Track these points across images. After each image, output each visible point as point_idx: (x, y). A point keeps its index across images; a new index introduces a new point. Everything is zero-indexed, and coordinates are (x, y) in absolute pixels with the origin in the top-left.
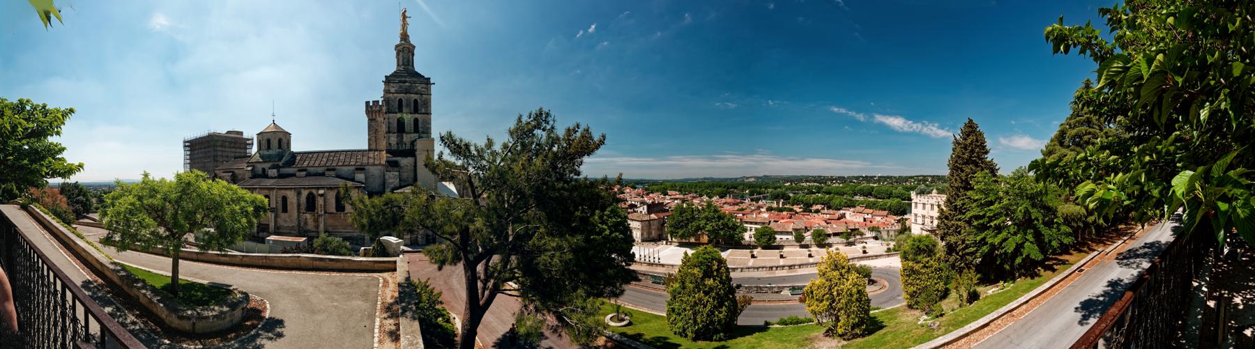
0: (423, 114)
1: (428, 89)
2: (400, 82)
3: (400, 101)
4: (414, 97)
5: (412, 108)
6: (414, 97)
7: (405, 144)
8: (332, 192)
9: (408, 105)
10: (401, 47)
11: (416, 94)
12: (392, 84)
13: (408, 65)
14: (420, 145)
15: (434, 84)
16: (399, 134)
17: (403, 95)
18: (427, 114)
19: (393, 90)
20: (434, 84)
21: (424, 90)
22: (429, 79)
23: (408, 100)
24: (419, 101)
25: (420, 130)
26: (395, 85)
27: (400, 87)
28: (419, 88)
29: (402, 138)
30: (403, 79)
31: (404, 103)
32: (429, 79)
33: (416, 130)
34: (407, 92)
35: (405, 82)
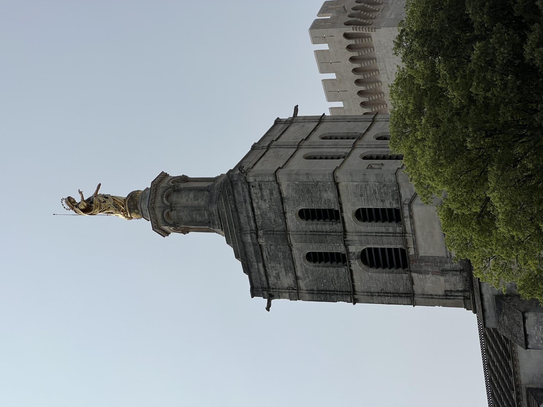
3: (312, 257)
12: (272, 280)
17: (295, 252)
19: (287, 281)
21: (266, 193)
25: (389, 204)
26: (272, 273)
28: (265, 206)
30: (251, 250)
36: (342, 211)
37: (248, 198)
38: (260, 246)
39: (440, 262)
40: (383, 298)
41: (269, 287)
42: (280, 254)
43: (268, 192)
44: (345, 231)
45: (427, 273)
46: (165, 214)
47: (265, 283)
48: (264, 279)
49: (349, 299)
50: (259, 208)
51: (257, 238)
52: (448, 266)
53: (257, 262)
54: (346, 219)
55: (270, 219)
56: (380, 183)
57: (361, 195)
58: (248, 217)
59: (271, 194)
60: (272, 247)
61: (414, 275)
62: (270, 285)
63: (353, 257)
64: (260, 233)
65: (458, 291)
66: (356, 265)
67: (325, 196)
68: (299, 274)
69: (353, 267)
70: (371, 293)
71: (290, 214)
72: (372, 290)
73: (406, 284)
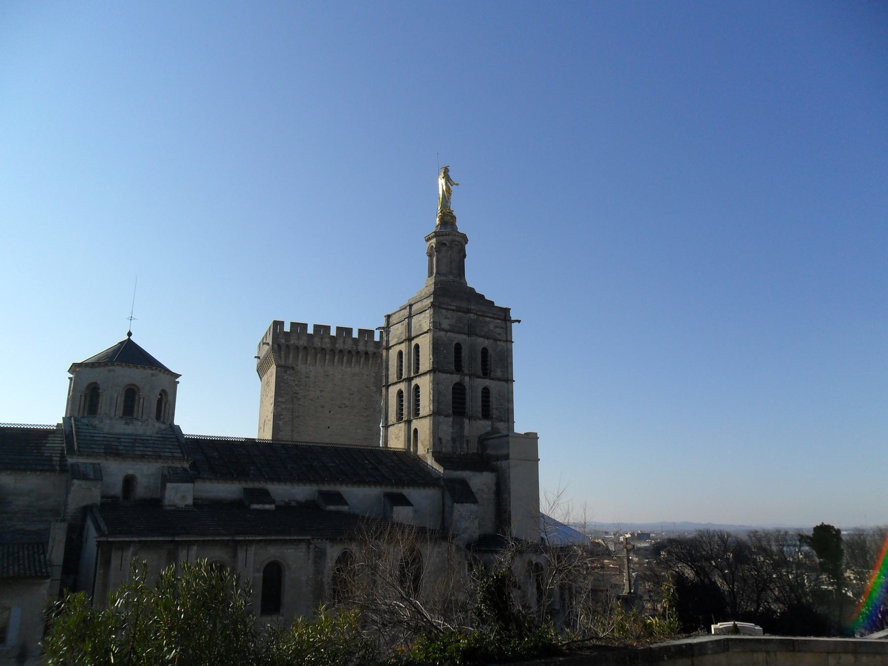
0: (499, 380)
1: (508, 331)
2: (459, 309)
3: (458, 347)
4: (482, 342)
6: (482, 342)
11: (486, 337)
12: (444, 311)
15: (519, 321)
17: (464, 337)
20: (519, 321)
21: (499, 330)
22: (507, 310)
24: (490, 351)
25: (495, 413)
26: (449, 314)
28: (492, 327)
29: (462, 427)
31: (465, 353)
32: (507, 310)
34: (471, 332)
35: (468, 311)
37: (496, 316)
41: (440, 308)
43: (500, 332)
44: (479, 377)
45: (453, 429)
46: (457, 243)
47: (442, 306)
54: (485, 380)
57: (499, 396)
59: (499, 334)
61: (451, 419)
62: (441, 309)
63: (461, 378)
66: (456, 378)
67: (499, 370)
68: (449, 334)
69: (455, 376)
71: (487, 342)
73: (445, 411)
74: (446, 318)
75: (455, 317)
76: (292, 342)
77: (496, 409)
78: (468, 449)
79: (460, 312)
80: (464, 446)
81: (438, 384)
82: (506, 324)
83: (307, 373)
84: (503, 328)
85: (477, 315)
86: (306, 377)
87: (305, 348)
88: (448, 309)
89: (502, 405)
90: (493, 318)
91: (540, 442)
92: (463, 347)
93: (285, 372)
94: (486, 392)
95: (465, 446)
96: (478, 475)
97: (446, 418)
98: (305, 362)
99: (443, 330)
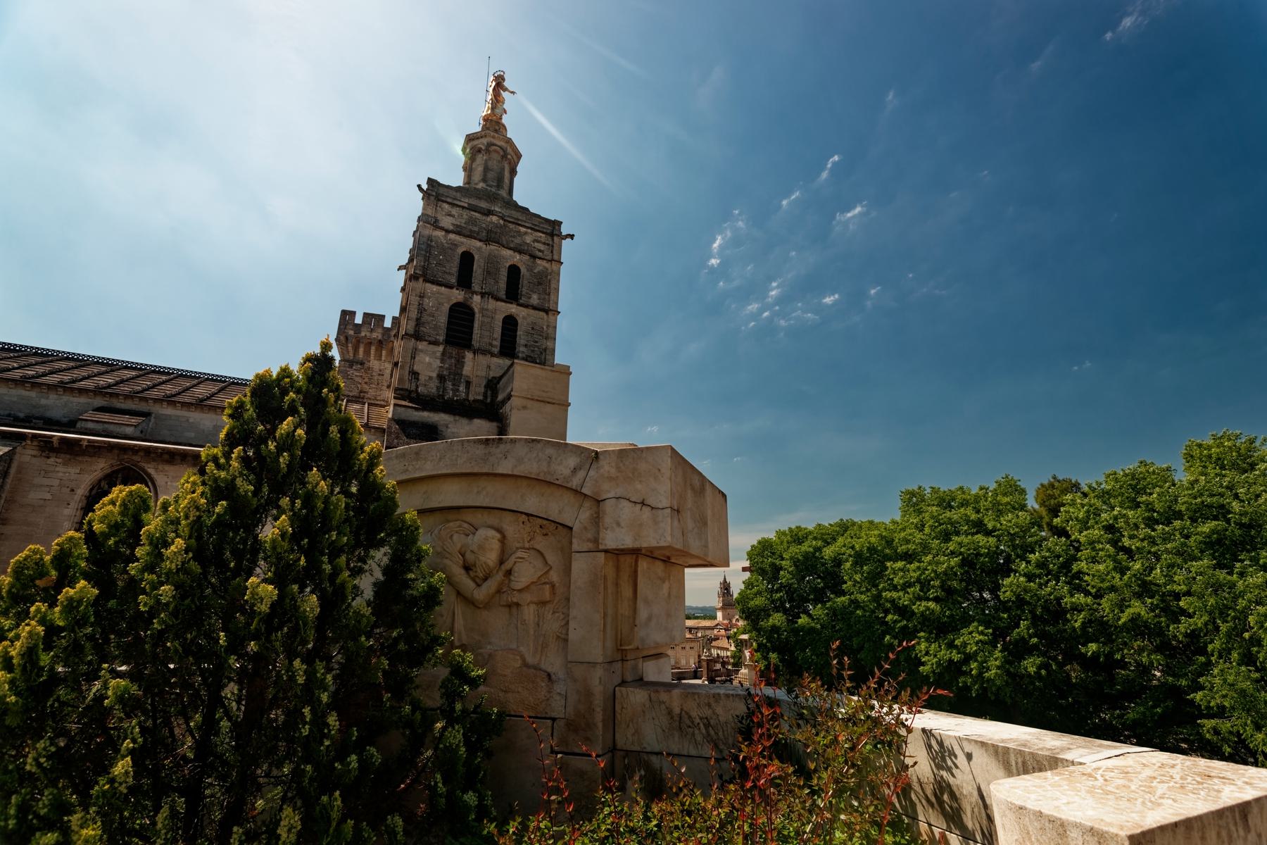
0: (535, 308)
2: (472, 208)
4: (510, 257)
5: (503, 284)
7: (468, 384)
8: (73, 471)
9: (490, 272)
10: (485, 141)
12: (446, 206)
13: (499, 186)
14: (523, 377)
15: (572, 237)
16: (454, 351)
17: (479, 244)
18: (547, 311)
19: (447, 222)
20: (572, 237)
21: (541, 247)
23: (492, 261)
24: (523, 270)
25: (521, 350)
26: (455, 211)
27: (472, 221)
28: (528, 239)
29: (460, 362)
30: (483, 205)
32: (556, 224)
33: (508, 348)
34: (490, 237)
35: (489, 213)
36: (519, 305)
37: (536, 228)
38: (488, 215)
39: (454, 379)
40: (416, 306)
41: (439, 200)
42: (476, 229)
44: (497, 299)
45: (442, 361)
48: (449, 200)
49: (418, 272)
50: (526, 233)
51: (498, 216)
52: (449, 385)
53: (469, 204)
54: (508, 305)
55: (514, 237)
56: (545, 350)
57: (533, 328)
58: (518, 220)
59: (540, 251)
60: (484, 226)
61: (441, 348)
62: (440, 203)
64: (502, 222)
65: (417, 387)
66: (458, 295)
67: (535, 296)
68: (452, 236)
69: (454, 290)
70: (423, 297)
72: (426, 300)
74: (449, 215)
75: (465, 216)
76: (363, 334)
77: (526, 346)
78: (467, 394)
79: (476, 211)
80: (461, 389)
81: (420, 297)
82: (553, 240)
83: (380, 371)
84: (548, 245)
85: (505, 220)
86: (379, 375)
87: (380, 342)
88: (453, 205)
89: (537, 342)
90: (532, 229)
91: (573, 380)
92: (476, 257)
93: (351, 366)
94: (510, 324)
95: (462, 388)
96: (464, 421)
97: (431, 346)
98: (379, 357)
99: (442, 229)
